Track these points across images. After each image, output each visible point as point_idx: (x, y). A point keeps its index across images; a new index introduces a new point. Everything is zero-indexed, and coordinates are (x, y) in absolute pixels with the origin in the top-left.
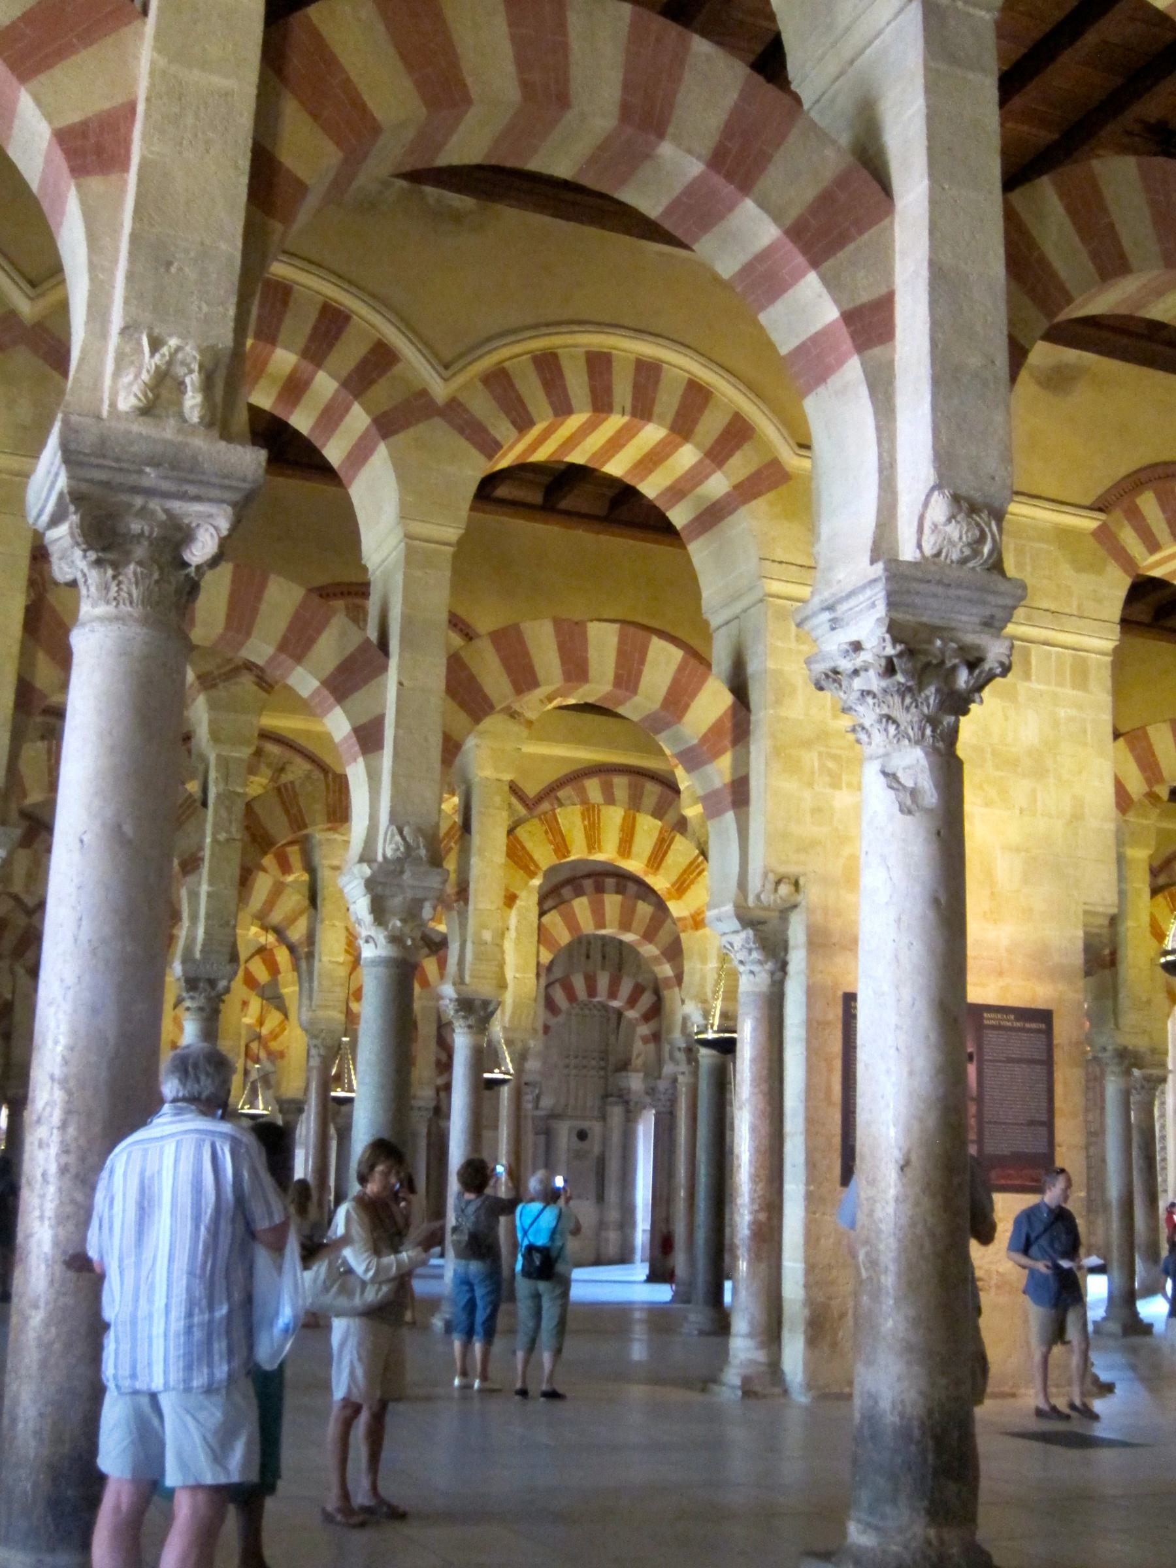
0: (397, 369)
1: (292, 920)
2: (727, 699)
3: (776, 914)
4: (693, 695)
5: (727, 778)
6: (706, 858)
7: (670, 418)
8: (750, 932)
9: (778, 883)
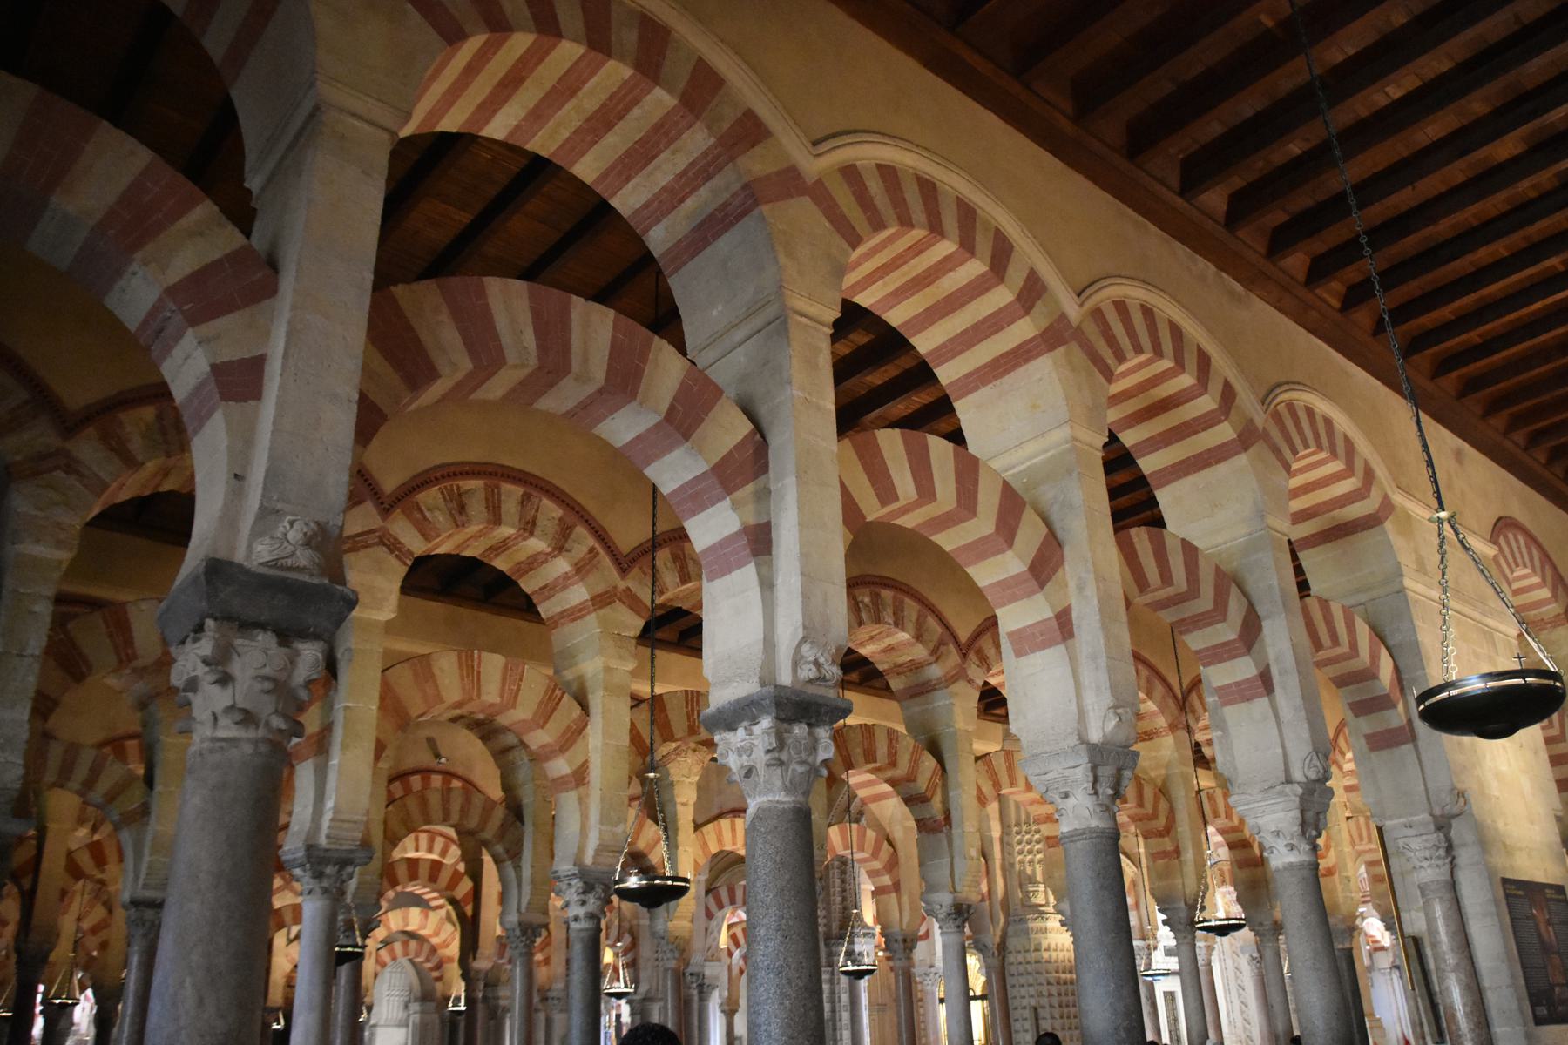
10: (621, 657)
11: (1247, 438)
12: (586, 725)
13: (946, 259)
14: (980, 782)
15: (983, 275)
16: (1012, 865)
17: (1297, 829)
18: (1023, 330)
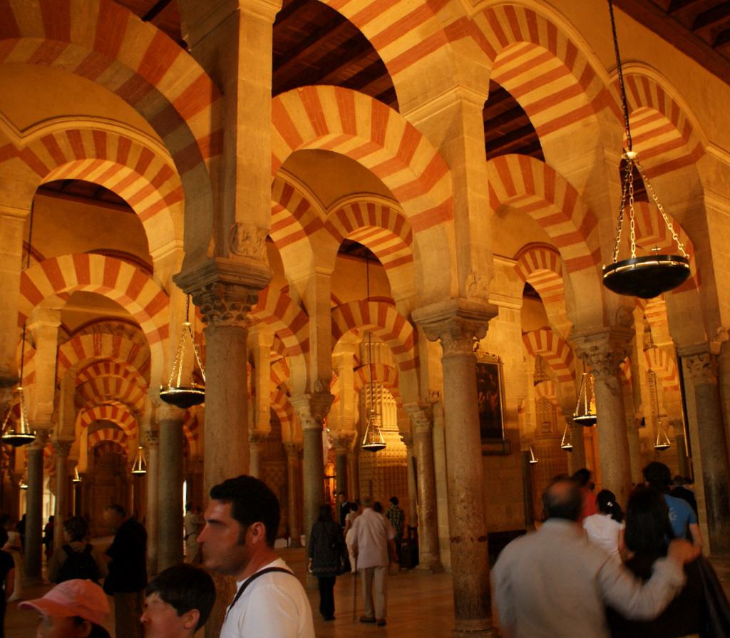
0: (310, 209)
1: (138, 399)
2: (411, 328)
3: (430, 405)
4: (401, 328)
5: (413, 357)
6: (338, 375)
7: (393, 227)
8: (423, 412)
9: (433, 394)
10: (52, 321)
11: (308, 230)
12: (34, 355)
13: (113, 167)
14: (277, 372)
15: (132, 173)
16: (364, 405)
17: (309, 414)
18: (156, 196)
